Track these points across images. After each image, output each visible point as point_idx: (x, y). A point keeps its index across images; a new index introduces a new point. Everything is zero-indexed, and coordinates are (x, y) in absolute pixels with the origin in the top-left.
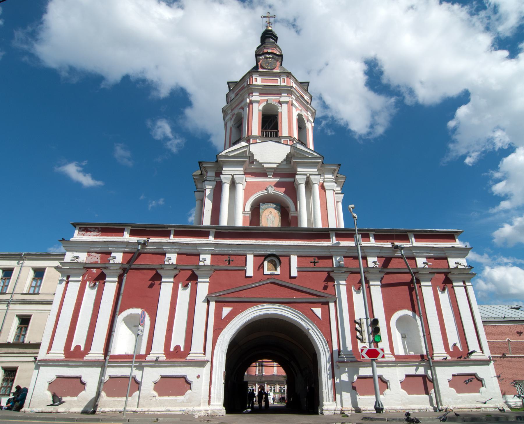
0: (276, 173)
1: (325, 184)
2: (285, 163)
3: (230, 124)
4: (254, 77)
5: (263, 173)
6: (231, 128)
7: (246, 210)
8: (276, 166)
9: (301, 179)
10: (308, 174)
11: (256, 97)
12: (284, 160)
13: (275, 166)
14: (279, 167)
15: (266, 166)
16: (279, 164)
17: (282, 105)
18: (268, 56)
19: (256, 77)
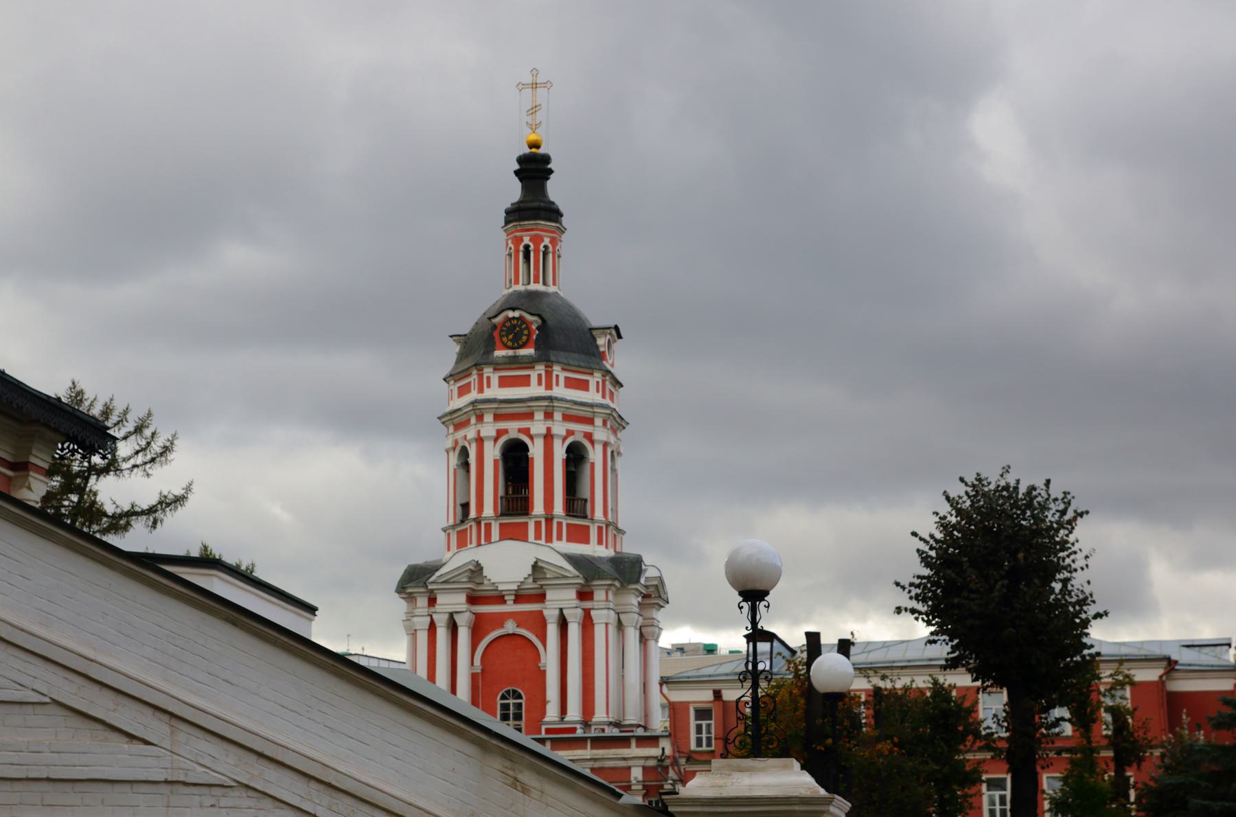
0: (519, 598)
1: (593, 613)
2: (531, 580)
3: (454, 459)
4: (485, 376)
5: (500, 599)
6: (455, 470)
7: (475, 664)
8: (516, 588)
9: (551, 614)
10: (561, 606)
11: (489, 428)
12: (529, 575)
13: (515, 587)
14: (523, 587)
15: (501, 588)
16: (522, 582)
17: (535, 440)
18: (511, 314)
19: (488, 375)
